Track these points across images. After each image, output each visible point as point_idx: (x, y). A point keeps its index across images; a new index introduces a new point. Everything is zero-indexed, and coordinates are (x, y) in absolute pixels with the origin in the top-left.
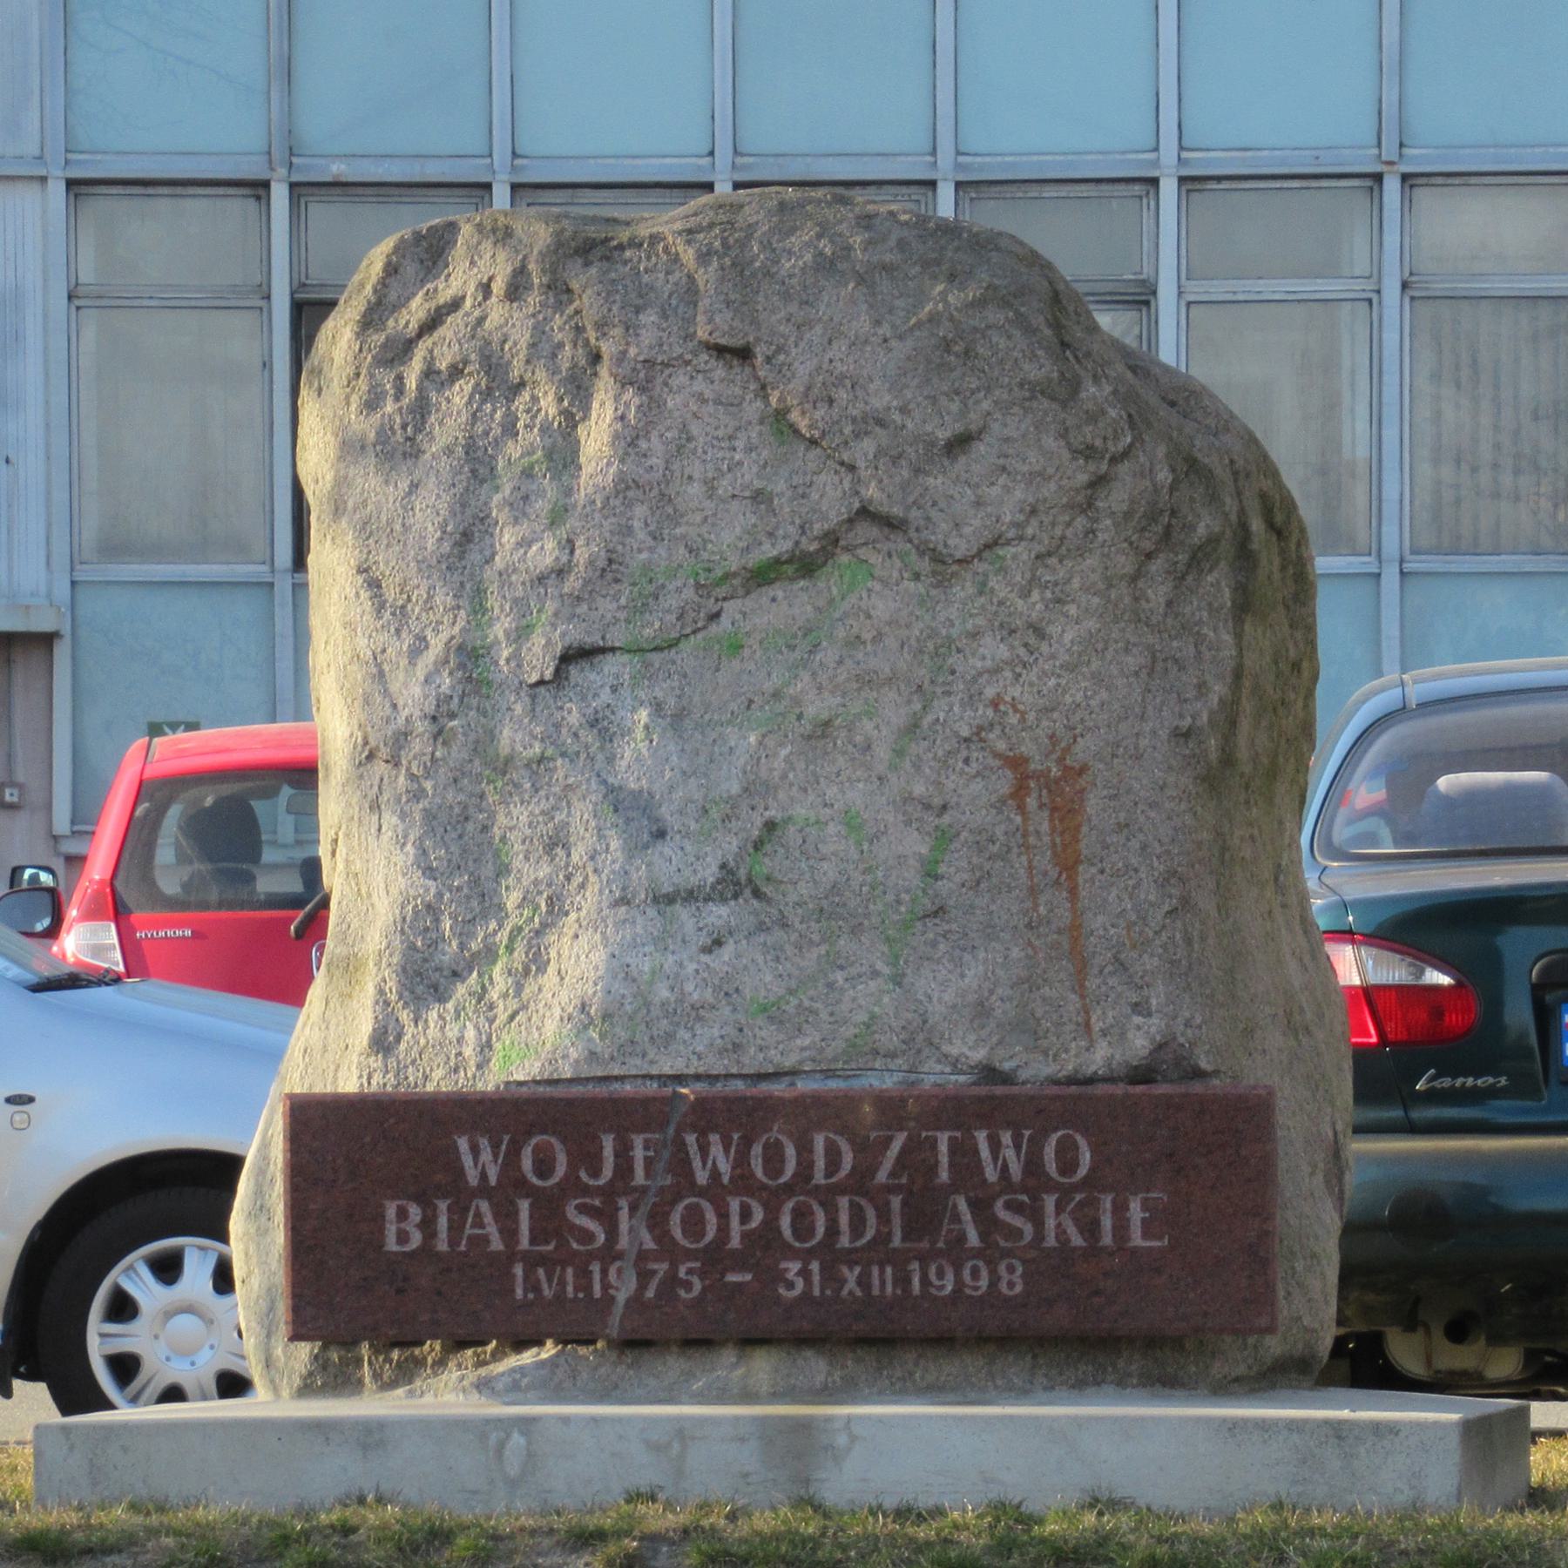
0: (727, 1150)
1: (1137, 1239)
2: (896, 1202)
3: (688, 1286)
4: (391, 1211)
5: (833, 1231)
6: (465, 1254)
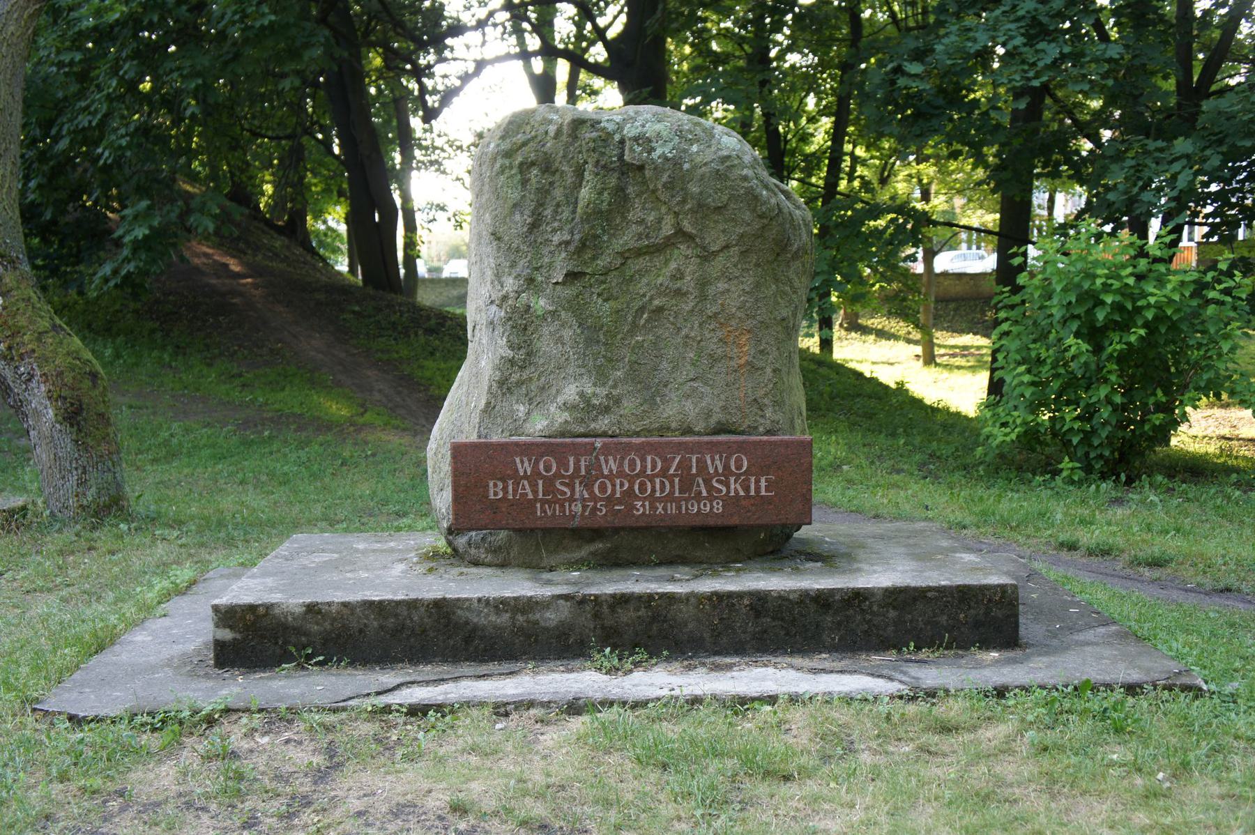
1: (763, 493)
2: (677, 480)
3: (601, 511)
4: (491, 484)
5: (653, 490)
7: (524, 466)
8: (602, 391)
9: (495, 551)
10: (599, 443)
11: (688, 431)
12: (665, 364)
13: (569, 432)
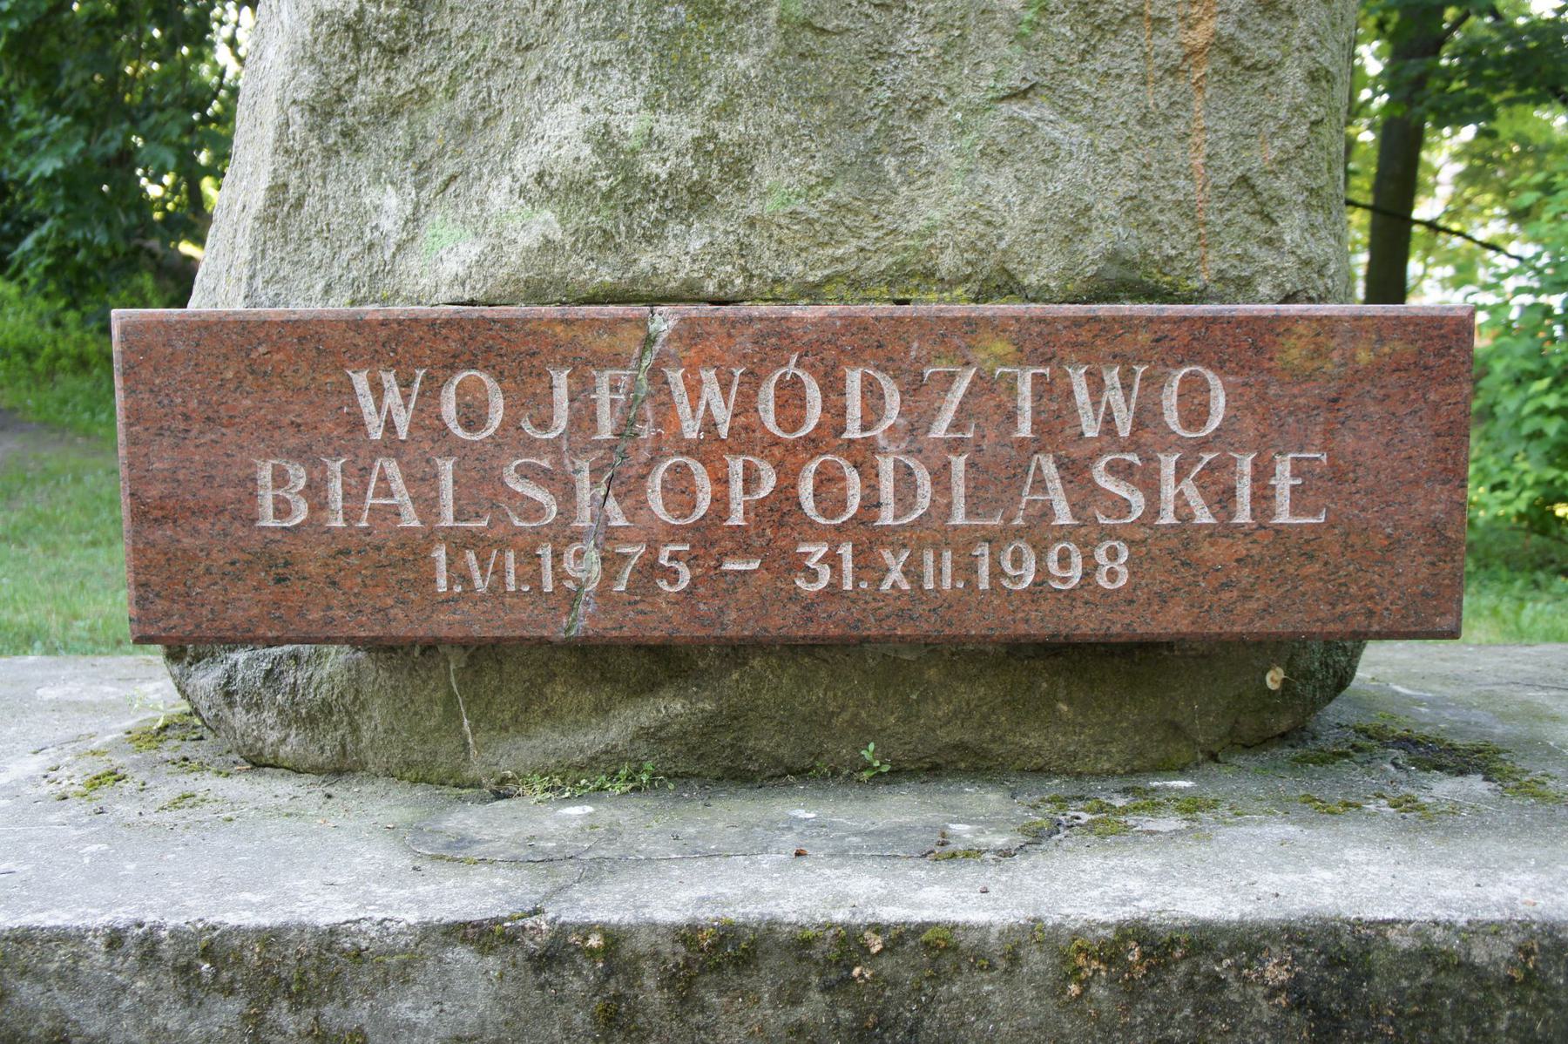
0: (725, 387)
1: (1283, 516)
2: (959, 463)
4: (265, 474)
6: (367, 532)
7: (383, 404)
8: (681, 129)
9: (313, 718)
10: (664, 321)
11: (1006, 285)
12: (912, 38)
13: (560, 282)
